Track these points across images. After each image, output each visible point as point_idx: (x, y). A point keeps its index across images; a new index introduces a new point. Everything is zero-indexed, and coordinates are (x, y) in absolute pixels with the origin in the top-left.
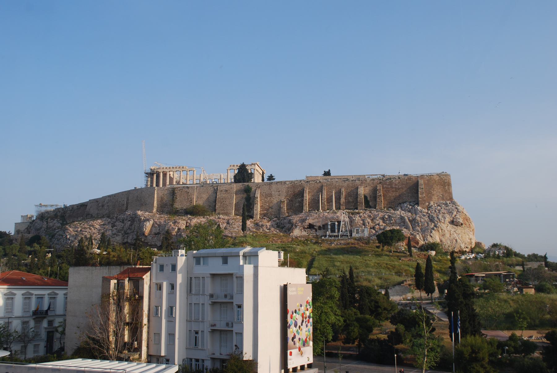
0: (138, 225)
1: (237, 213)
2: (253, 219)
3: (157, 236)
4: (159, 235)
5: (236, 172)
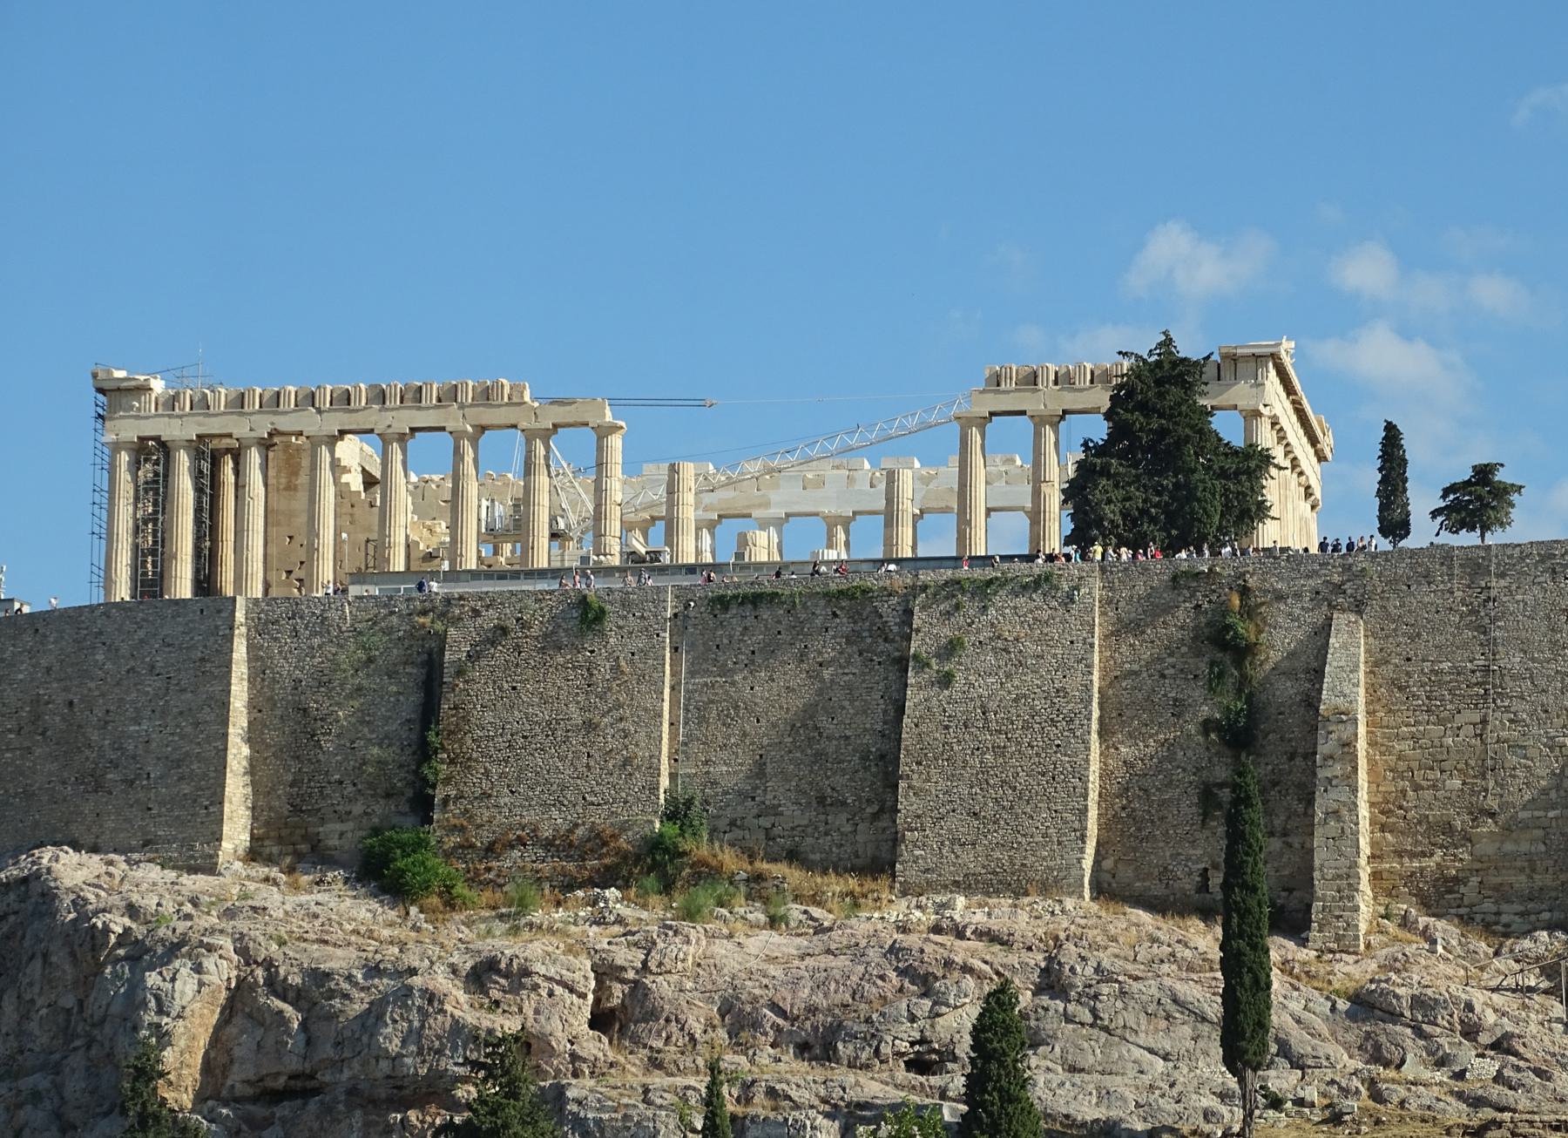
0: (69, 1001)
1: (1126, 873)
2: (1303, 943)
3: (283, 1110)
4: (313, 1104)
5: (1099, 430)
